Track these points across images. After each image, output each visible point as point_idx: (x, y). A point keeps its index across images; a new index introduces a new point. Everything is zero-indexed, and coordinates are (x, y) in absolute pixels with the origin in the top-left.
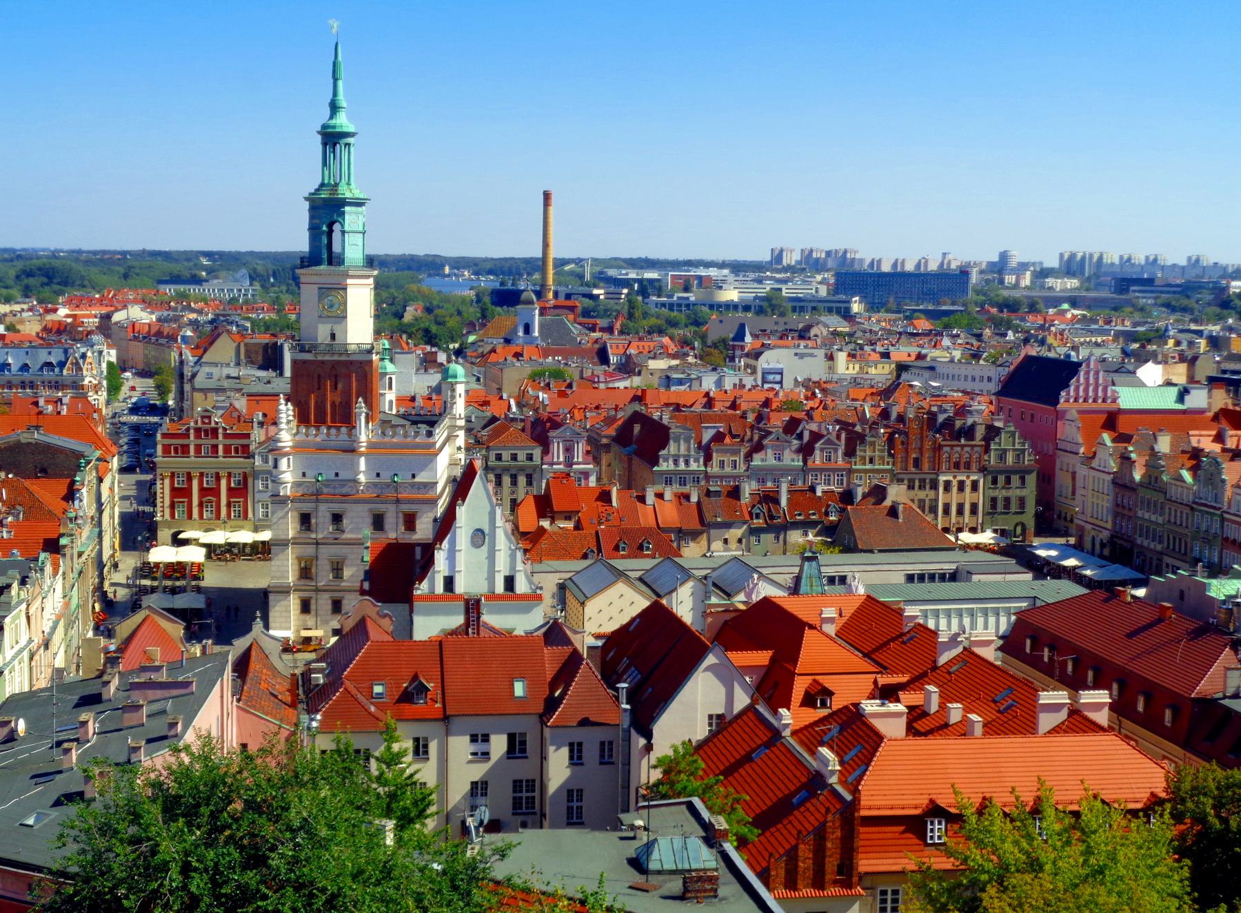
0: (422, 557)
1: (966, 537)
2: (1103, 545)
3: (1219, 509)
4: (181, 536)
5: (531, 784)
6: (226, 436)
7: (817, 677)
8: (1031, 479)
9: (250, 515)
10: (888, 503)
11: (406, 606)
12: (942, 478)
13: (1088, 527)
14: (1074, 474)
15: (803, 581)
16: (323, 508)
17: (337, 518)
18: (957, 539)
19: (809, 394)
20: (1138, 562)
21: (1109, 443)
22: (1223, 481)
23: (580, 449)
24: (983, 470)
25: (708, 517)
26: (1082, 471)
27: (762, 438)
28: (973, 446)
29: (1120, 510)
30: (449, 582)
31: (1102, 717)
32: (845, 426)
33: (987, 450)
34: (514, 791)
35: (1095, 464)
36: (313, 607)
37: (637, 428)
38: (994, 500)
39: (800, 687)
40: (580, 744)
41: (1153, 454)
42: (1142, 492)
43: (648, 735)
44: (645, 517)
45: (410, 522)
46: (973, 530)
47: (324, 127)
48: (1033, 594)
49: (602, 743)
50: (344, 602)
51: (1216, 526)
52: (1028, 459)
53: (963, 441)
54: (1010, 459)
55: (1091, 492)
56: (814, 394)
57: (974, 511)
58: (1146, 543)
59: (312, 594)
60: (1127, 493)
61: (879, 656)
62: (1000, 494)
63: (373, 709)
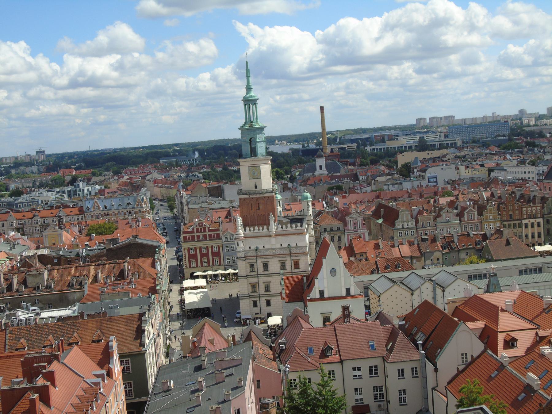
0: (307, 281)
1: (538, 248)
4: (195, 274)
5: (381, 388)
7: (508, 333)
9: (222, 263)
11: (302, 303)
15: (491, 287)
17: (266, 266)
18: (534, 249)
19: (453, 187)
23: (360, 222)
24: (542, 217)
25: (423, 250)
27: (440, 211)
28: (536, 207)
30: (322, 292)
32: (475, 202)
33: (543, 208)
34: (374, 391)
36: (258, 304)
39: (501, 338)
40: (402, 370)
44: (395, 253)
46: (540, 245)
47: (244, 97)
49: (412, 369)
50: (271, 301)
53: (531, 204)
56: (455, 187)
57: (539, 236)
59: (258, 299)
61: (535, 321)
63: (309, 360)
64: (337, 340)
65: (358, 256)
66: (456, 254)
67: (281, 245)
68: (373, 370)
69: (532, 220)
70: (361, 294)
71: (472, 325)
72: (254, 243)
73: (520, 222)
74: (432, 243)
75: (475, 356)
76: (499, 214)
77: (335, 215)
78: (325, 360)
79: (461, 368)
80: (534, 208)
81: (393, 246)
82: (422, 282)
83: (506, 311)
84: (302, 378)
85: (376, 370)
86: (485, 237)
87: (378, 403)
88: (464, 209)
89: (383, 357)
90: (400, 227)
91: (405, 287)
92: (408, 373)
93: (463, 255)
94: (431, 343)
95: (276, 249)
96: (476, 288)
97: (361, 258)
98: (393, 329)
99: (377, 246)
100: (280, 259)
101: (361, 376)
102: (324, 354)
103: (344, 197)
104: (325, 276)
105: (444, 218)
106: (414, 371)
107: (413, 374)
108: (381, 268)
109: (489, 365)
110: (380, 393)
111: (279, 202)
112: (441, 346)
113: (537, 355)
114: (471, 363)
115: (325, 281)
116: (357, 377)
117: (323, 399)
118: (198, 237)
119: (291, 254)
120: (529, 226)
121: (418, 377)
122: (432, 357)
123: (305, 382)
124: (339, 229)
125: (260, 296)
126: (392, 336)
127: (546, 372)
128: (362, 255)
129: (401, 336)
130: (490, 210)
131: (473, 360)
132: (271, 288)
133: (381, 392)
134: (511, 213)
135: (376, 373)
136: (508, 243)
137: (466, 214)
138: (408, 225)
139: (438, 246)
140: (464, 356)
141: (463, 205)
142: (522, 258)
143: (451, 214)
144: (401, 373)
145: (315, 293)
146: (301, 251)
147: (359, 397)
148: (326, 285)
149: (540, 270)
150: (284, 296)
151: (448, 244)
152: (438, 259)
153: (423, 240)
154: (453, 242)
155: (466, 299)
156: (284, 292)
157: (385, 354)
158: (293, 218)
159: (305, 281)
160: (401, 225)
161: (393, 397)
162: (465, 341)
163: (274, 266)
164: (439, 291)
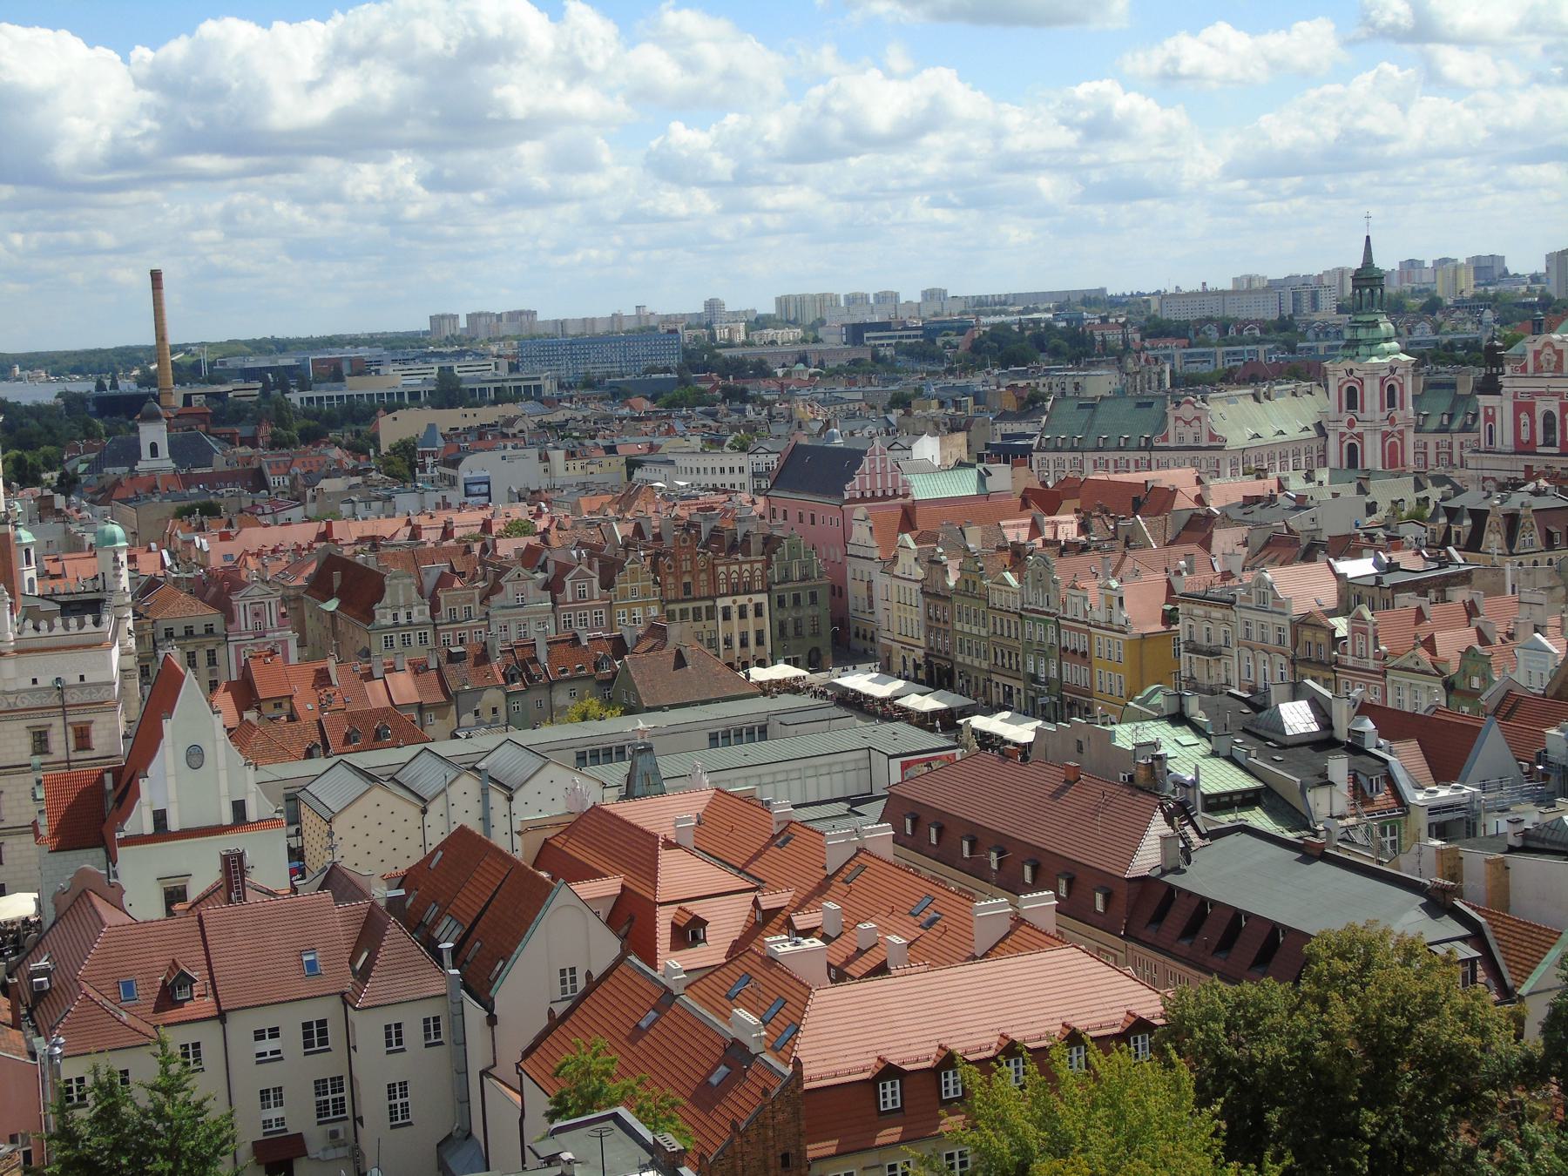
0: (116, 783)
1: (758, 674)
2: (917, 667)
3: (1053, 615)
5: (337, 1083)
11: (101, 852)
13: (896, 646)
14: (870, 582)
18: (748, 676)
19: (534, 509)
20: (959, 682)
21: (912, 545)
22: (1055, 582)
23: (274, 609)
24: (768, 589)
25: (453, 686)
26: (880, 581)
27: (499, 575)
28: (752, 562)
29: (934, 624)
30: (160, 817)
31: (1049, 922)
32: (594, 550)
34: (318, 1094)
35: (898, 571)
37: (337, 575)
38: (782, 626)
39: (664, 920)
40: (398, 1026)
42: (957, 601)
43: (488, 1005)
44: (376, 696)
45: (83, 738)
46: (762, 664)
48: (866, 744)
49: (426, 1021)
51: (1052, 633)
53: (740, 556)
55: (896, 605)
56: (539, 509)
57: (760, 641)
58: (968, 661)
60: (941, 604)
62: (789, 615)
63: (125, 1017)
64: (207, 954)
65: (268, 709)
66: (542, 695)
67: (35, 681)
68: (315, 1034)
69: (742, 599)
70: (278, 816)
71: (588, 889)
73: (710, 603)
74: (476, 665)
75: (596, 975)
76: (655, 582)
77: (198, 589)
78: (173, 1015)
79: (559, 1009)
80: (745, 567)
81: (369, 676)
82: (452, 774)
83: (677, 846)
84: (103, 1071)
85: (323, 1033)
86: (619, 647)
87: (330, 1127)
89: (343, 994)
90: (389, 621)
91: (401, 792)
92: (413, 1034)
93: (561, 697)
94: (478, 944)
95: (18, 692)
96: (597, 788)
97: (277, 712)
98: (370, 912)
99: (322, 678)
100: (31, 722)
101: (278, 1052)
102: (168, 998)
103: (225, 537)
104: (170, 770)
105: (510, 596)
106: (432, 1026)
107: (427, 1037)
108: (335, 740)
109: (633, 996)
110: (334, 1098)
111: (27, 551)
112: (505, 951)
113: (758, 960)
114: (586, 994)
115: (171, 782)
116: (269, 1057)
117: (166, 1129)
119: (64, 708)
120: (735, 616)
121: (441, 1043)
122: (479, 986)
123: (112, 1084)
124: (209, 630)
126: (369, 934)
127: (780, 1004)
128: (280, 705)
129: (395, 933)
130: (633, 572)
131: (593, 985)
133: (338, 1095)
134: (687, 579)
135: (323, 1042)
136: (680, 661)
137: (568, 584)
138: (409, 615)
139: (494, 675)
140: (568, 976)
141: (560, 557)
142: (717, 701)
143: (530, 583)
144: (394, 1035)
145: (140, 820)
146: (96, 697)
147: (274, 1113)
148: (172, 795)
149: (763, 733)
150: (44, 831)
151: (522, 668)
152: (495, 710)
153: (453, 658)
154: (535, 660)
155: (572, 818)
156: (43, 821)
157: (348, 984)
158: (70, 598)
159: (109, 785)
160: (390, 617)
161: (373, 1104)
162: (568, 935)
164: (497, 798)
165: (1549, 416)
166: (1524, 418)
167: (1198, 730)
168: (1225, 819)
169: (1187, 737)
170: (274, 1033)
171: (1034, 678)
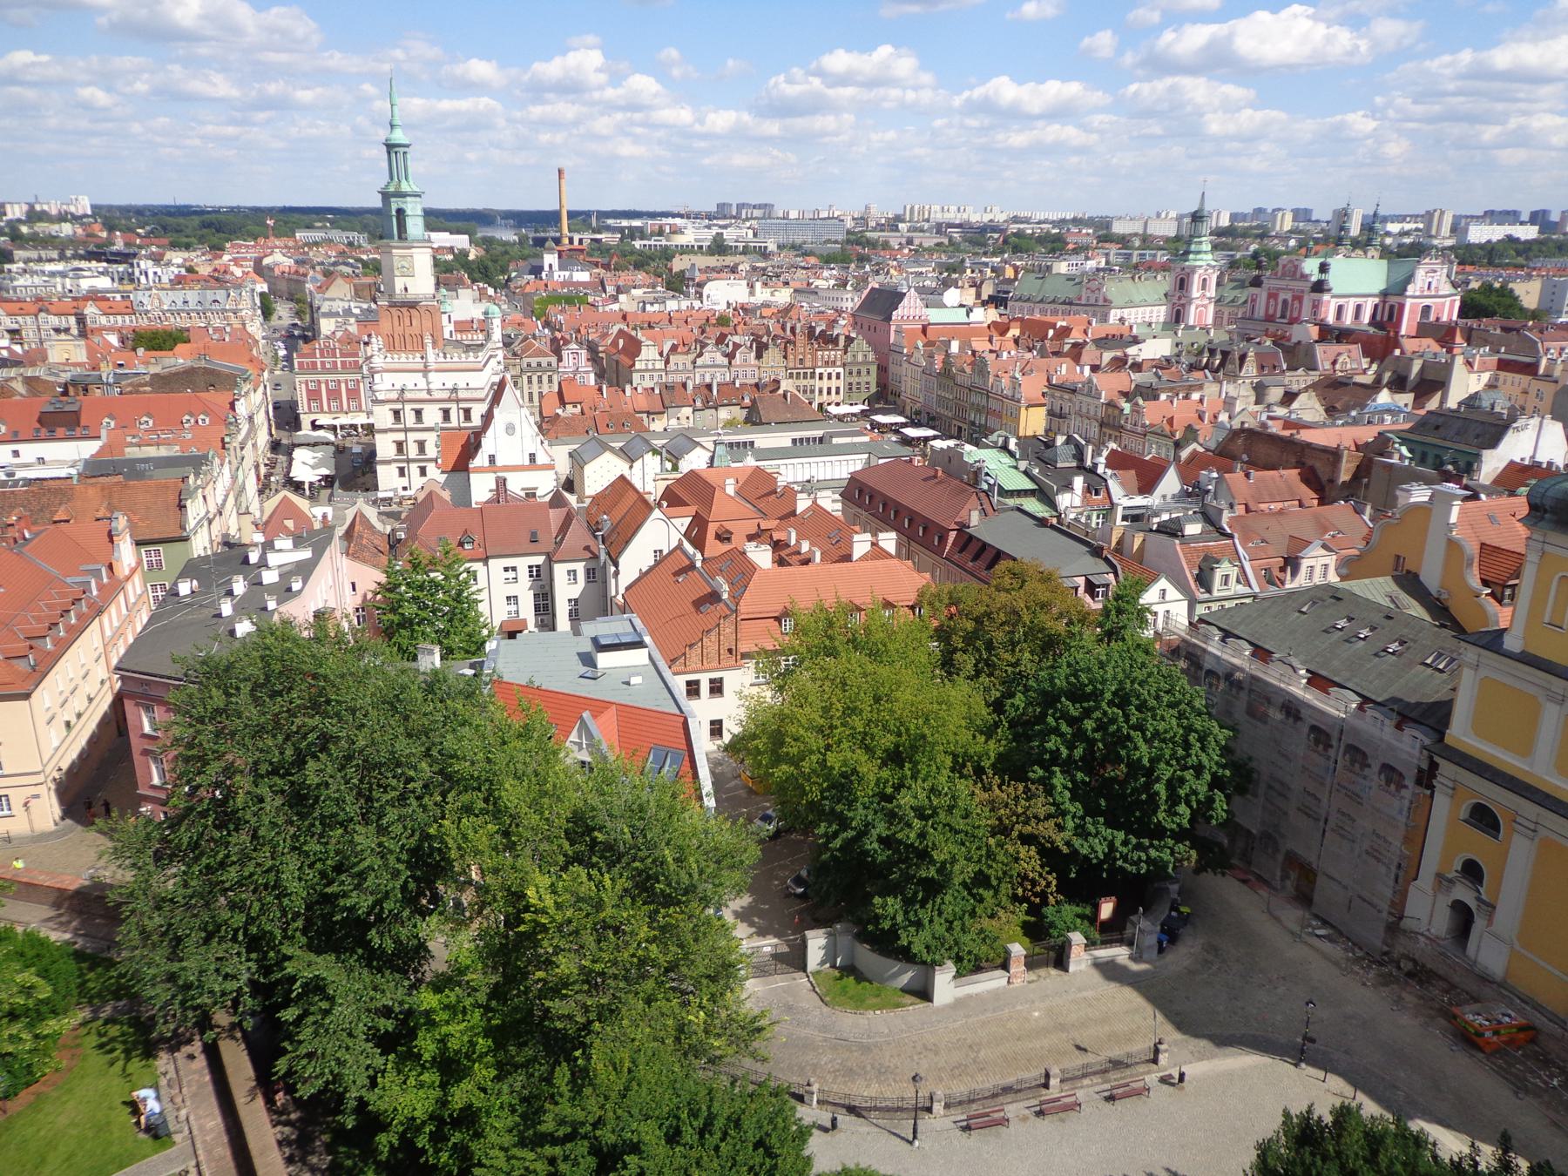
6: (342, 355)
8: (874, 369)
10: (781, 391)
12: (818, 371)
16: (408, 407)
17: (418, 413)
24: (844, 365)
25: (667, 403)
30: (492, 459)
37: (621, 342)
41: (948, 355)
43: (616, 565)
51: (984, 402)
52: (871, 357)
54: (860, 358)
57: (838, 392)
69: (830, 370)
72: (400, 380)
88: (737, 346)
106: (590, 574)
118: (323, 363)
119: (458, 401)
124: (550, 364)
125: (408, 461)
132: (427, 450)
141: (736, 339)
163: (432, 415)
165: (1285, 302)
166: (1272, 302)
167: (1012, 454)
168: (1011, 502)
169: (1007, 460)
170: (514, 569)
171: (973, 423)
